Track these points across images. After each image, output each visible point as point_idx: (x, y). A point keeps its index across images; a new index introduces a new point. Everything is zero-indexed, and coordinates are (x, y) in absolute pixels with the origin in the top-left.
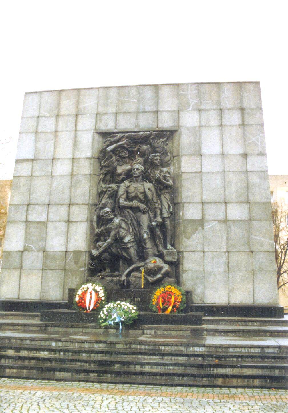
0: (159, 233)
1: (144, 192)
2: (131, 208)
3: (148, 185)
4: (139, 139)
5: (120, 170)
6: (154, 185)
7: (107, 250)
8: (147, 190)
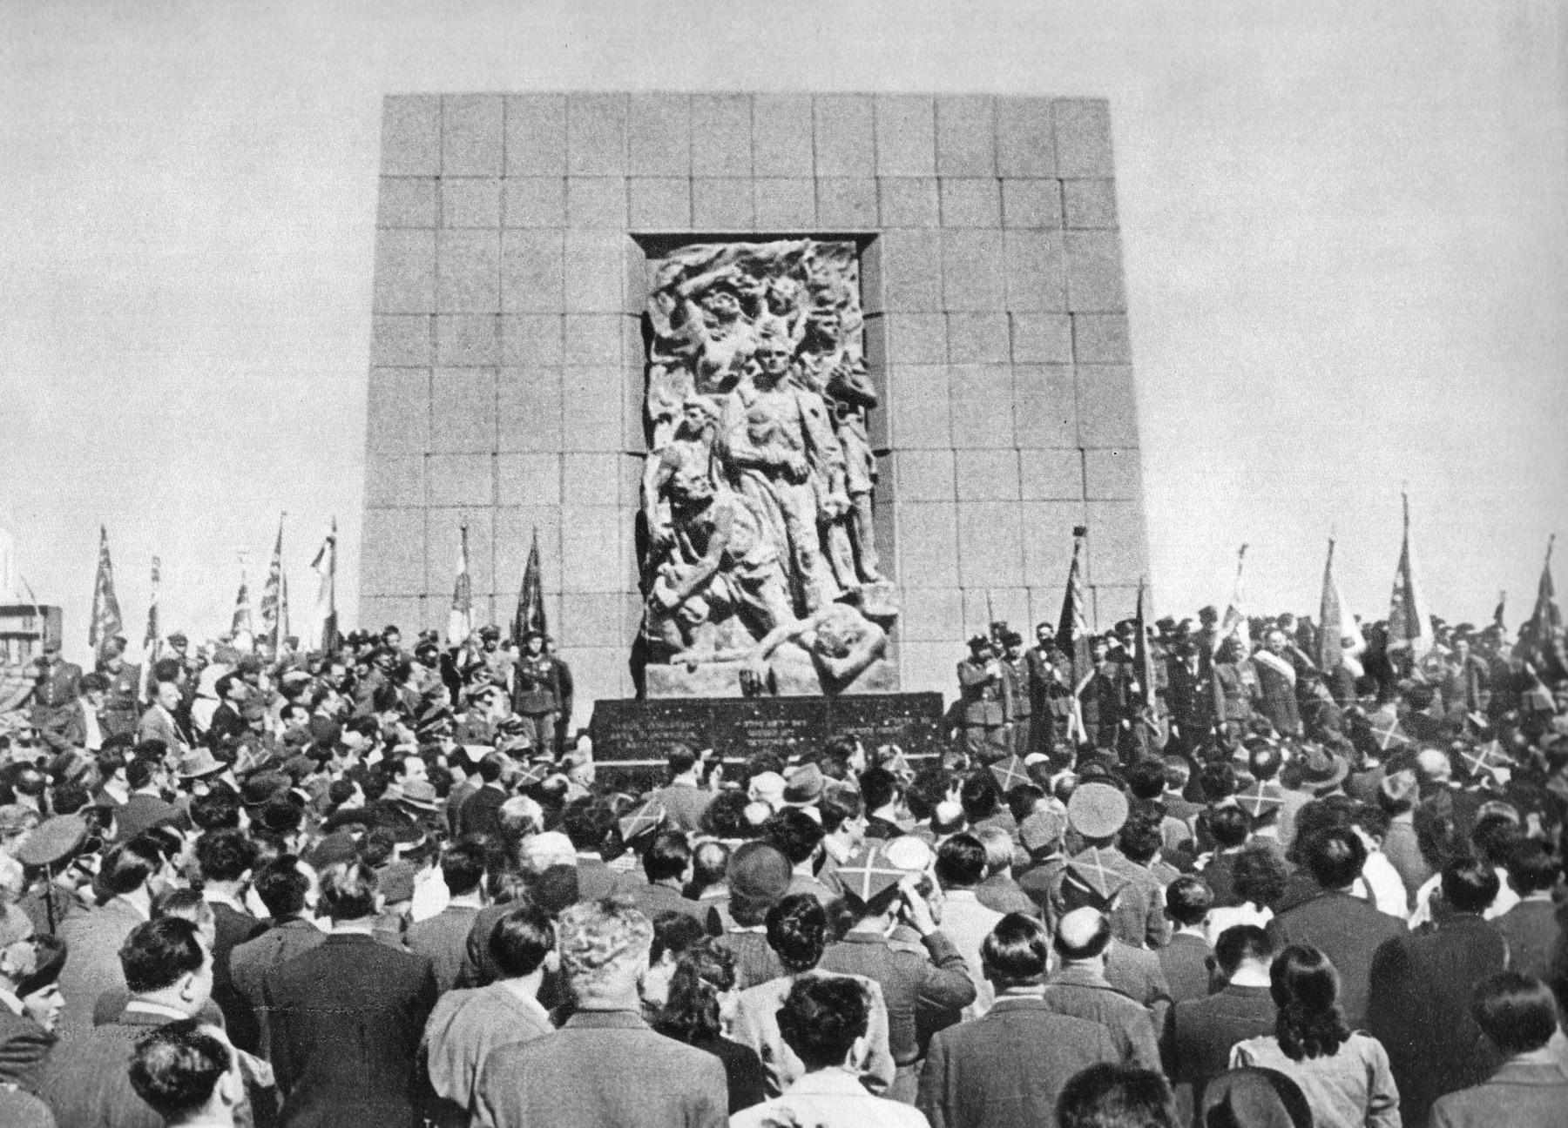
0: (838, 535)
1: (802, 420)
2: (762, 465)
3: (813, 401)
4: (771, 260)
5: (720, 353)
6: (826, 401)
7: (700, 587)
8: (807, 414)
